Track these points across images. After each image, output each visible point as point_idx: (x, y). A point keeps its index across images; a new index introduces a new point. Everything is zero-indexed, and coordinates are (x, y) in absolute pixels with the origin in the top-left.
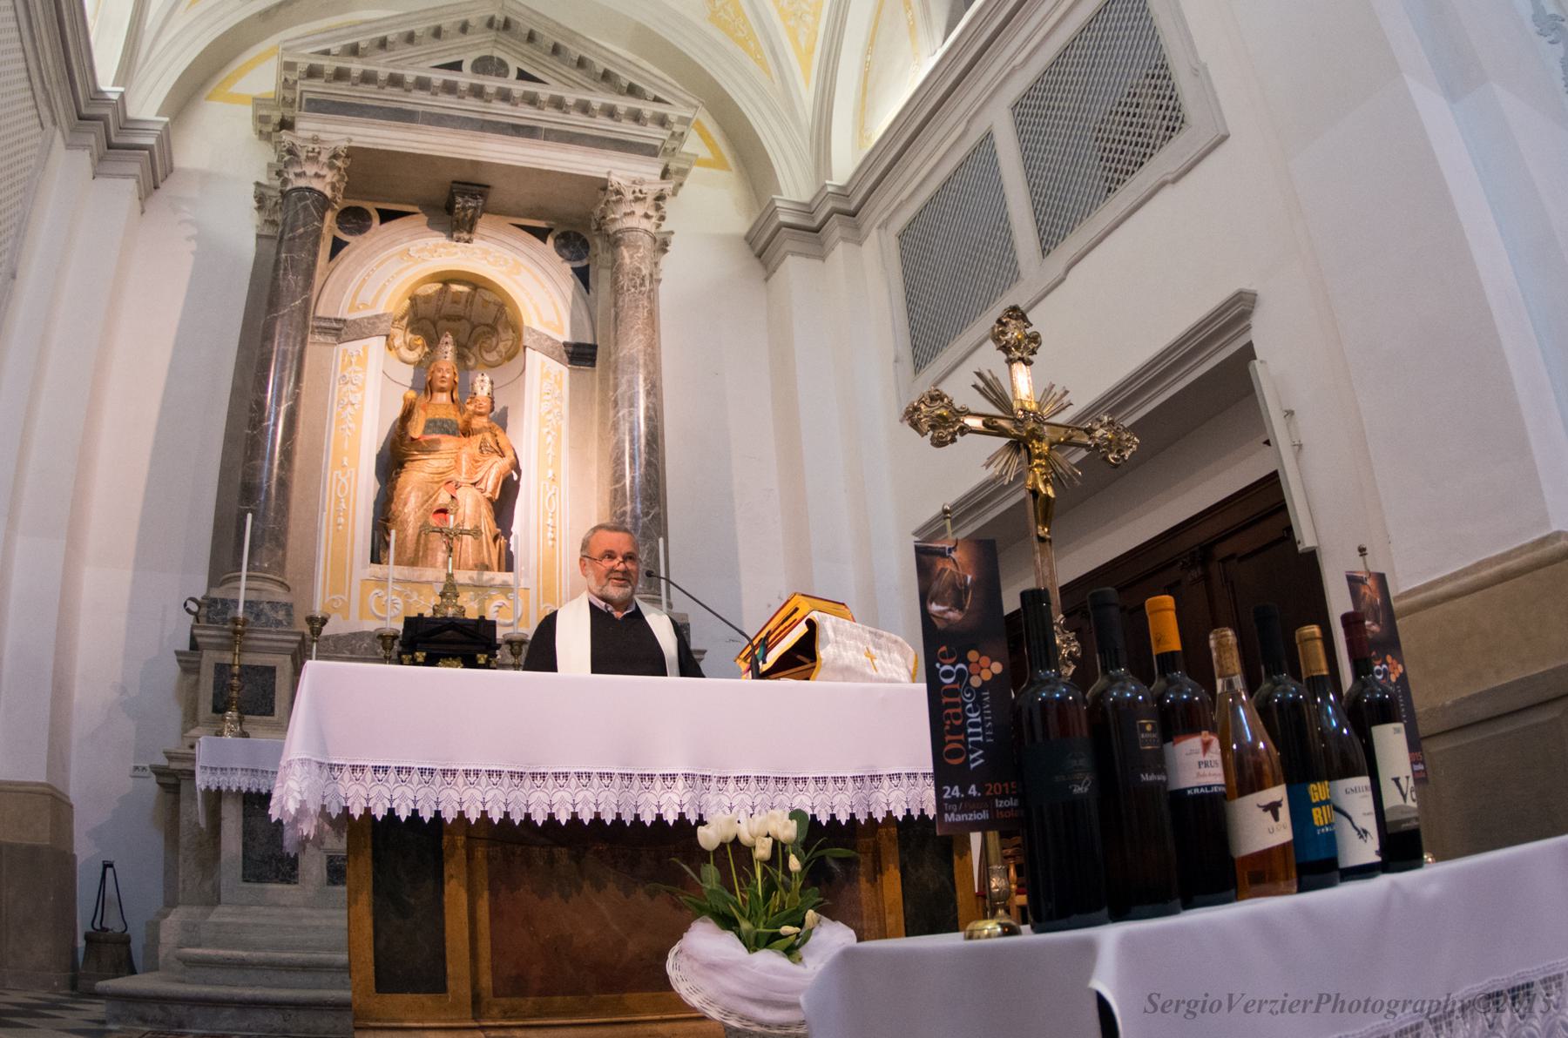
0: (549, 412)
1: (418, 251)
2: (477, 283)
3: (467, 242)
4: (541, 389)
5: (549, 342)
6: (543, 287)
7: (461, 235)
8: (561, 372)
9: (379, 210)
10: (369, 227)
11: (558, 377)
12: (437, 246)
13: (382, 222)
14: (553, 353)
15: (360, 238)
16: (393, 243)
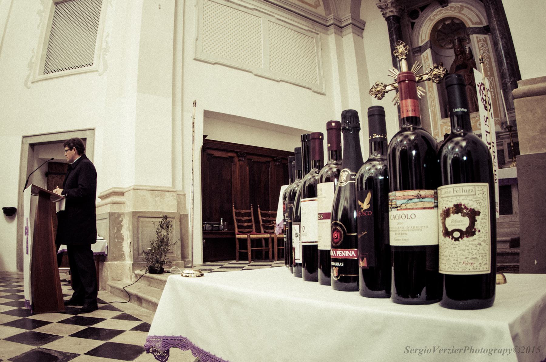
0: (484, 53)
1: (433, 16)
2: (452, 18)
3: (446, 6)
4: (479, 46)
5: (477, 29)
6: (472, 10)
7: (443, 5)
8: (485, 38)
9: (420, 8)
10: (419, 14)
11: (485, 40)
12: (438, 12)
13: (422, 12)
14: (480, 32)
15: (418, 19)
16: (426, 17)
